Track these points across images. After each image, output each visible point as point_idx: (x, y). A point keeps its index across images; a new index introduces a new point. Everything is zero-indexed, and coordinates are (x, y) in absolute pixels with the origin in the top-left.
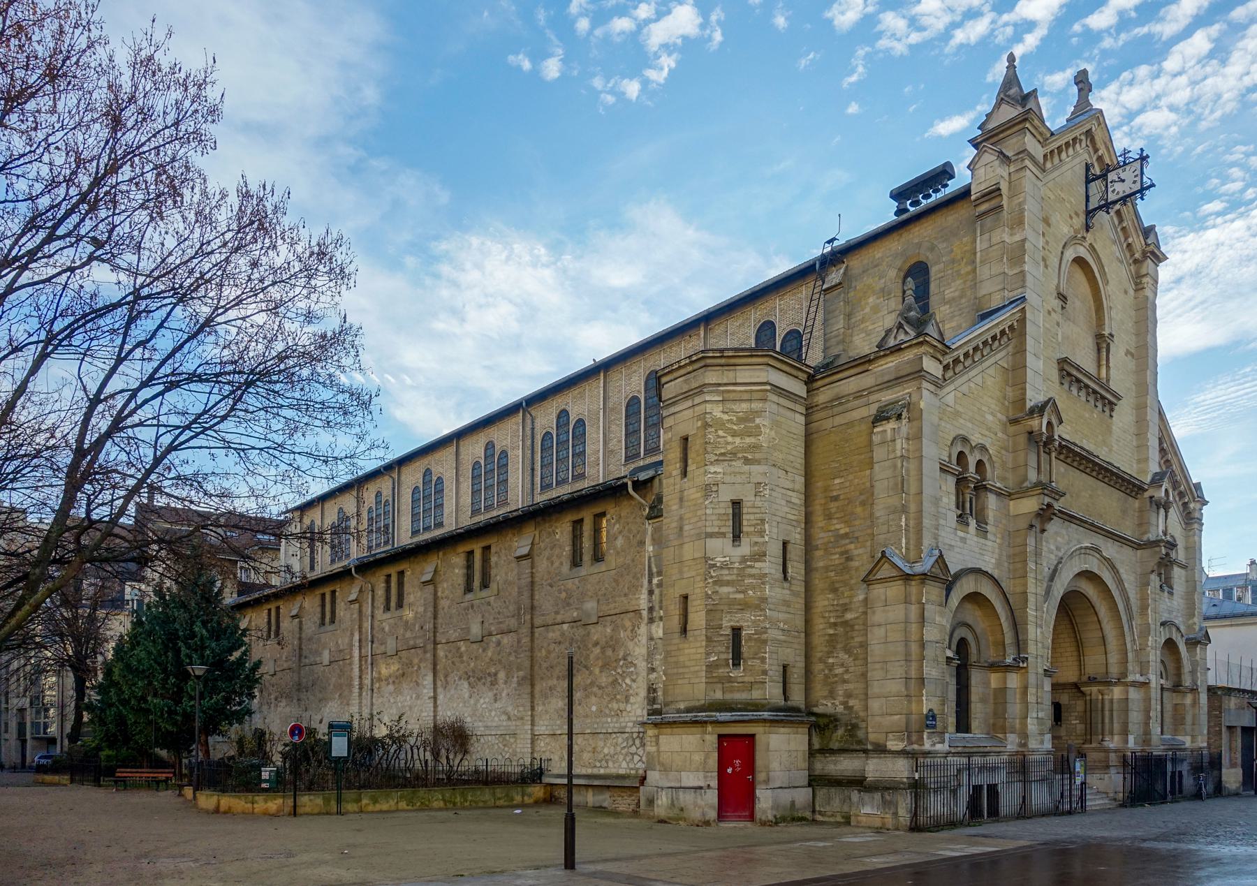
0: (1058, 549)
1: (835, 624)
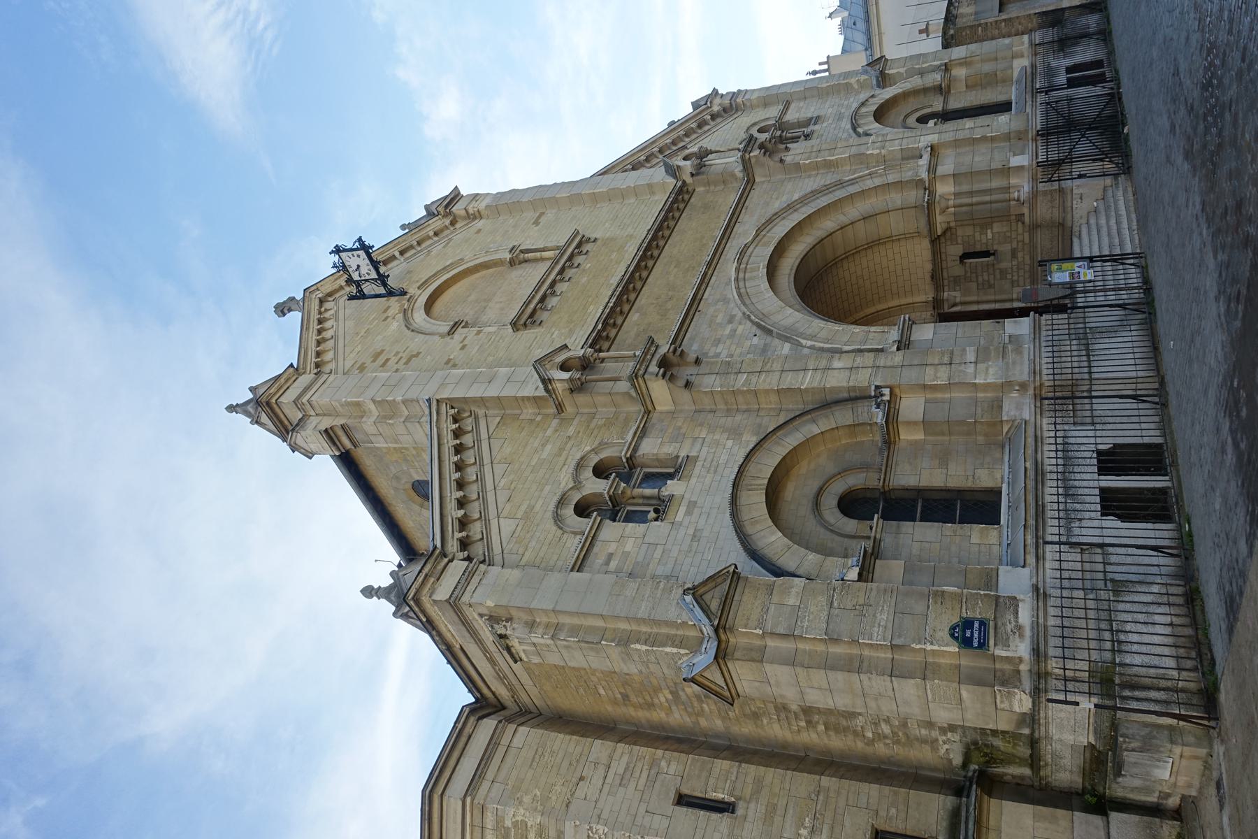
0: (731, 320)
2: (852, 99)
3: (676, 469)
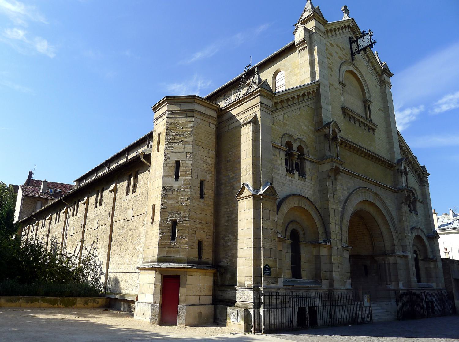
0: (349, 189)
1: (228, 220)
2: (423, 226)
3: (302, 174)
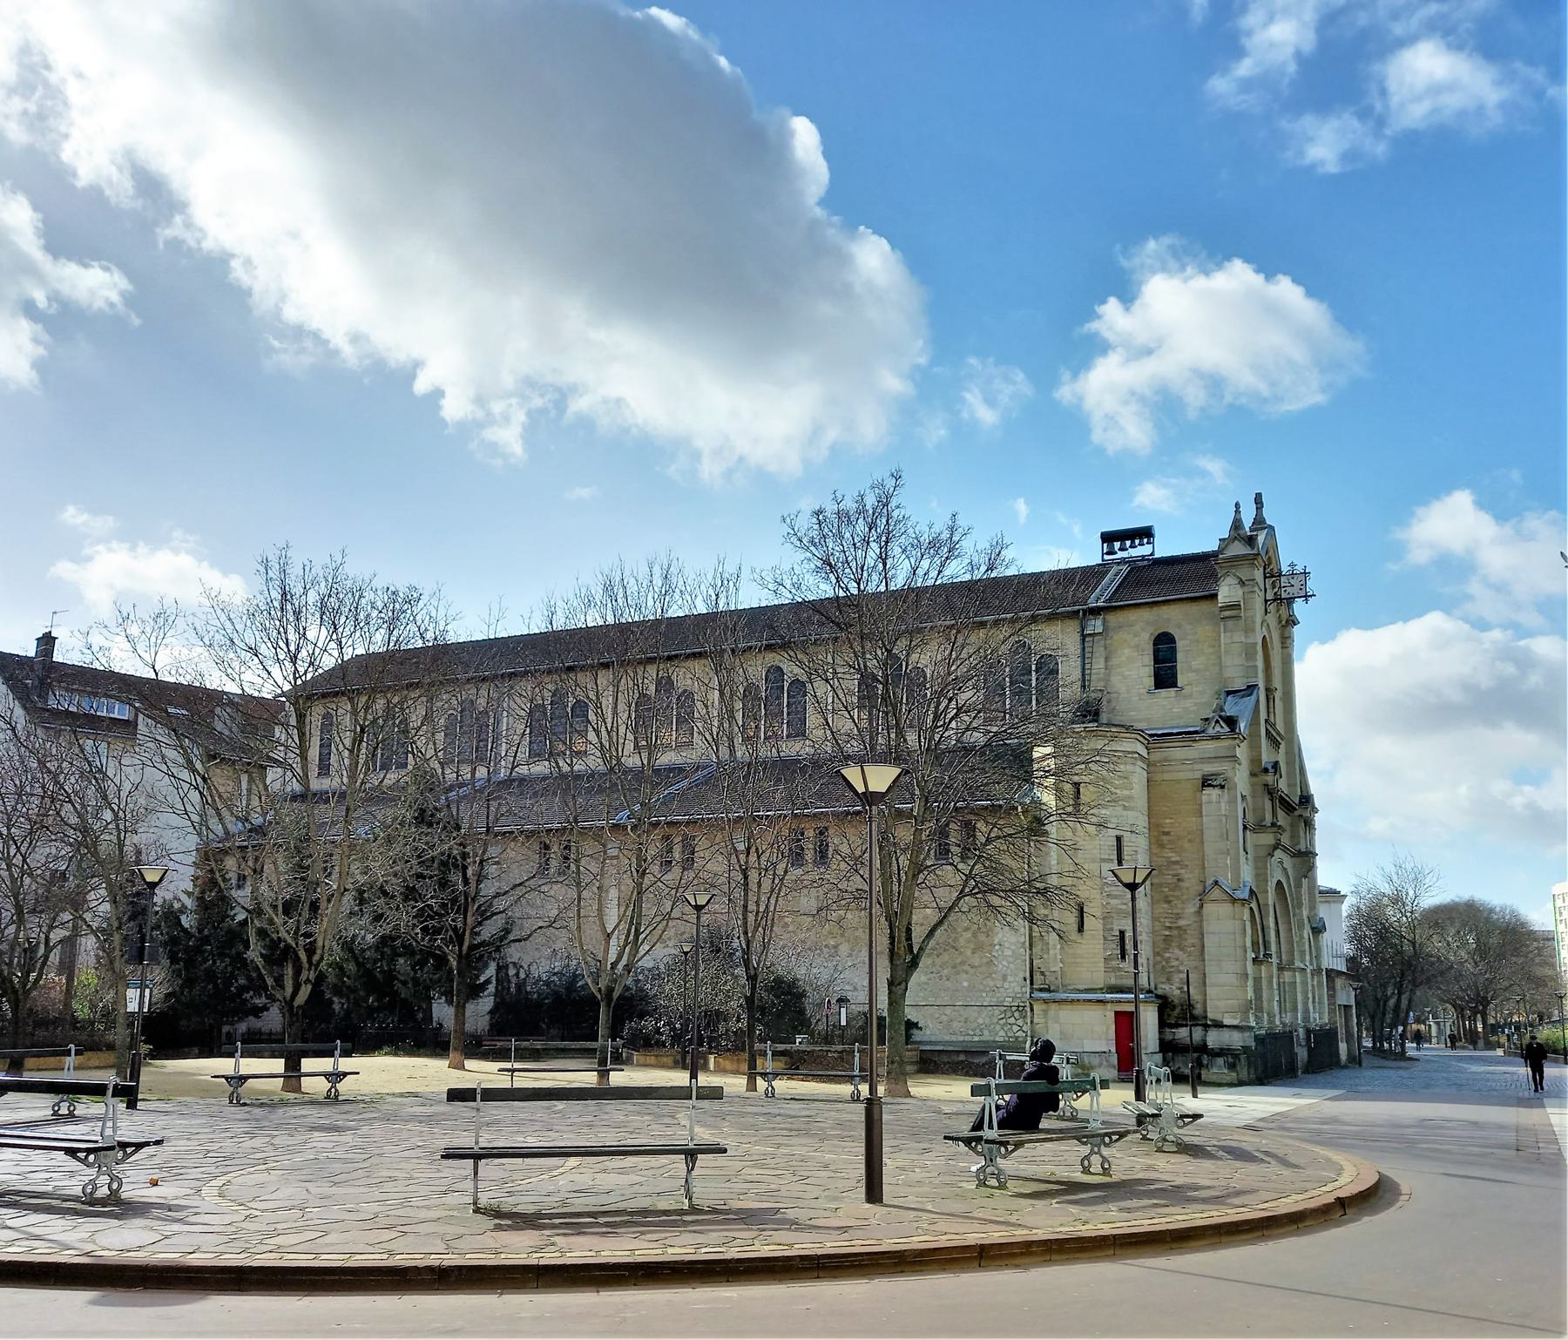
1: (1170, 928)
